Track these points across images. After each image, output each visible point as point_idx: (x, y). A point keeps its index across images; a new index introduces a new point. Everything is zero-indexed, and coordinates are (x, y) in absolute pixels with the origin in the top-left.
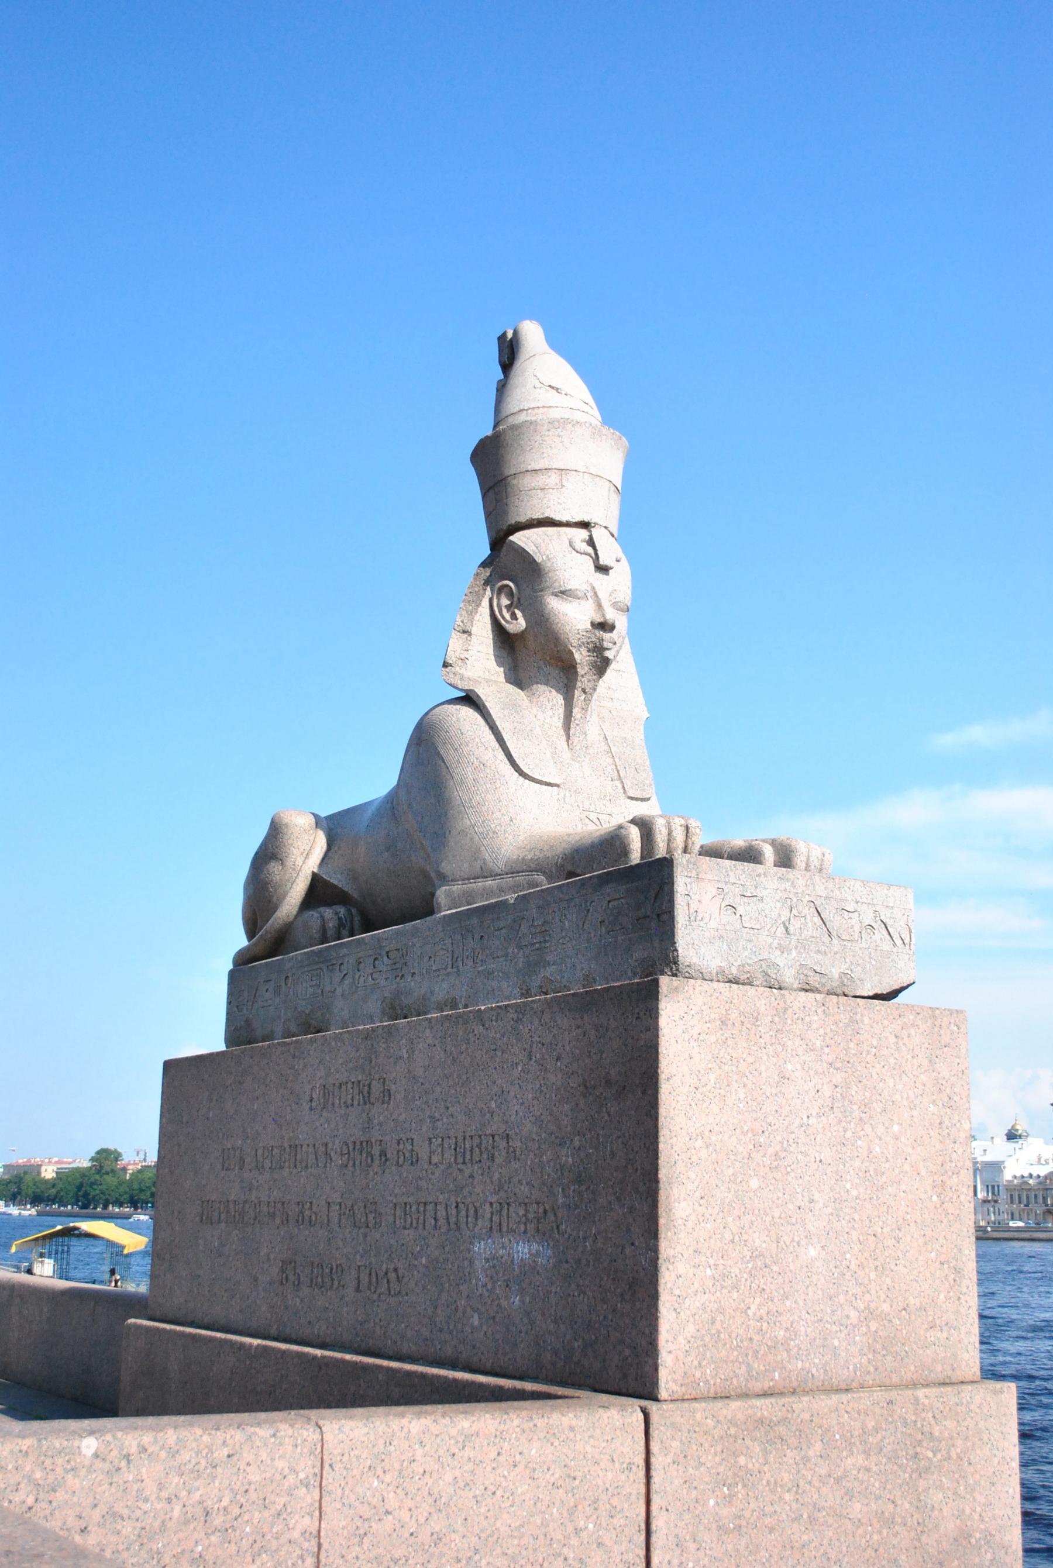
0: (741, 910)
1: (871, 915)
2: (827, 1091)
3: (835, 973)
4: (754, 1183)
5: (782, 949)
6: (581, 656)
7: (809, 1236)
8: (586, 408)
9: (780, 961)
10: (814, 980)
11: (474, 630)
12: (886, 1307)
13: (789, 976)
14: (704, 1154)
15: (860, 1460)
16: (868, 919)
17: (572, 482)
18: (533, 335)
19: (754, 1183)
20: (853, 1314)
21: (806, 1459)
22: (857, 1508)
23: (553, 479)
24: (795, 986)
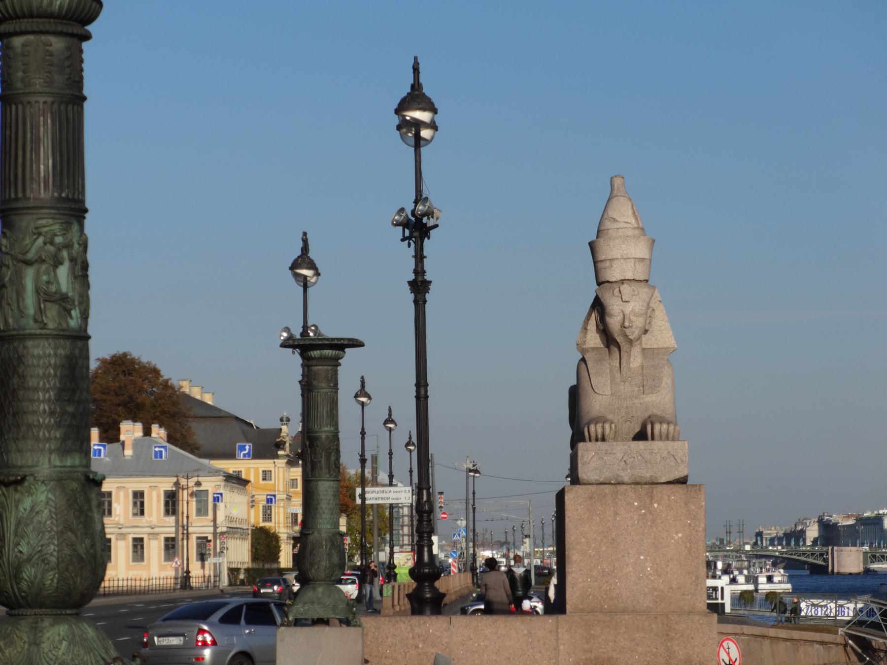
0: (605, 458)
1: (666, 453)
2: (636, 517)
3: (648, 475)
4: (604, 549)
5: (623, 470)
6: (619, 339)
7: (627, 565)
8: (626, 225)
9: (622, 473)
10: (638, 480)
11: (589, 328)
12: (662, 588)
13: (626, 479)
14: (583, 540)
15: (642, 635)
16: (665, 454)
17: (615, 264)
18: (618, 182)
19: (604, 549)
20: (646, 590)
21: (619, 633)
22: (640, 649)
23: (608, 264)
24: (629, 482)
